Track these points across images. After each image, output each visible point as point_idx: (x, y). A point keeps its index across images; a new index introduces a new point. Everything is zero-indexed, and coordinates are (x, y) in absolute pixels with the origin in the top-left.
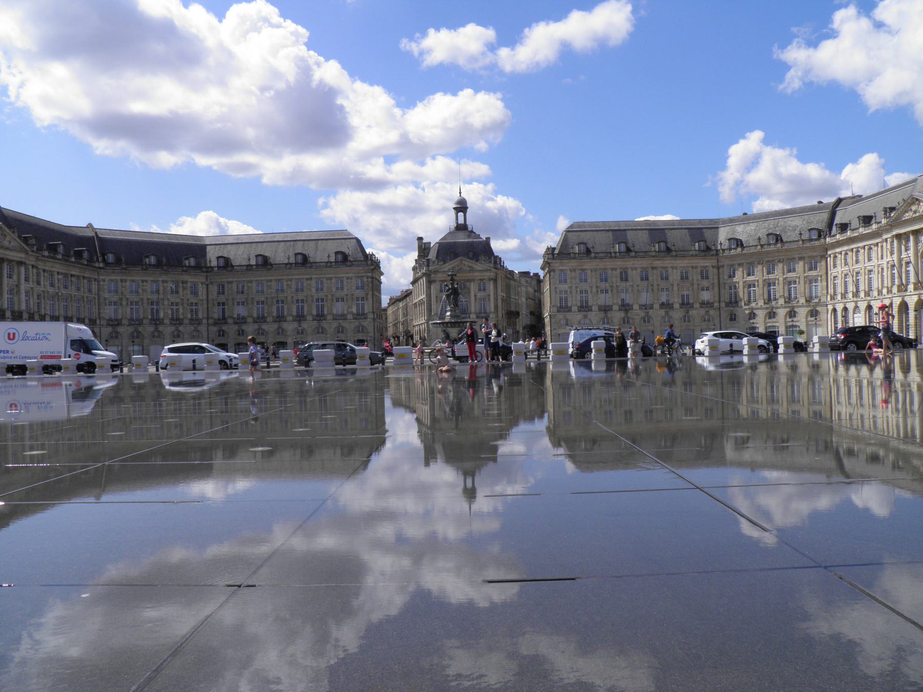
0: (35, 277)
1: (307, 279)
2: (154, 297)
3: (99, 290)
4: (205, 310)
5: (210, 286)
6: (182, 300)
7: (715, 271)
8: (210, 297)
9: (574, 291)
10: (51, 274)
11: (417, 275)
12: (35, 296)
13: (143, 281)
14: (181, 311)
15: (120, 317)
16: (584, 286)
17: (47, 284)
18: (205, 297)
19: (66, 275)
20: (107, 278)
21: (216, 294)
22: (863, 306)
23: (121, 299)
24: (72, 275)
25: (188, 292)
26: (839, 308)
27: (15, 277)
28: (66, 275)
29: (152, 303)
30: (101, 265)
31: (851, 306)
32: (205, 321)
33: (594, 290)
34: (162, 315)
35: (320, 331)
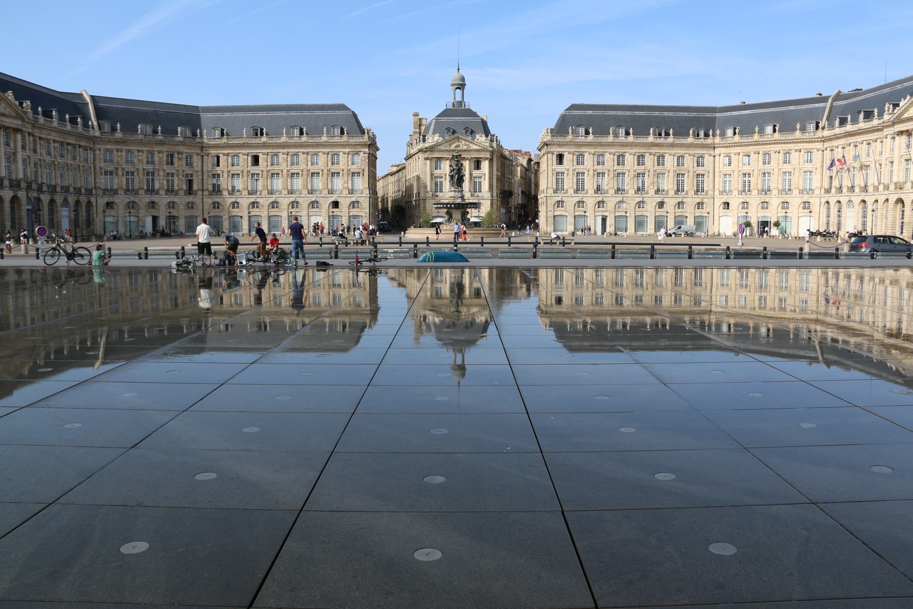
0: (32, 145)
1: (303, 153)
2: (150, 167)
3: (94, 159)
4: (200, 181)
5: (205, 157)
6: (178, 171)
7: (712, 158)
8: (205, 168)
9: (571, 172)
10: (48, 141)
11: (412, 152)
12: (32, 165)
13: (139, 151)
14: (176, 182)
15: (115, 187)
16: (580, 168)
17: (44, 152)
18: (200, 168)
19: (62, 144)
20: (103, 147)
21: (210, 166)
22: (856, 200)
23: (117, 169)
24: (68, 144)
25: (184, 163)
26: (833, 201)
27: (12, 145)
28: (62, 144)
29: (148, 174)
30: (97, 134)
31: (844, 200)
32: (200, 193)
33: (591, 173)
34: (157, 186)
35: (314, 204)
